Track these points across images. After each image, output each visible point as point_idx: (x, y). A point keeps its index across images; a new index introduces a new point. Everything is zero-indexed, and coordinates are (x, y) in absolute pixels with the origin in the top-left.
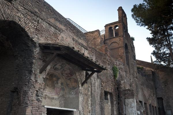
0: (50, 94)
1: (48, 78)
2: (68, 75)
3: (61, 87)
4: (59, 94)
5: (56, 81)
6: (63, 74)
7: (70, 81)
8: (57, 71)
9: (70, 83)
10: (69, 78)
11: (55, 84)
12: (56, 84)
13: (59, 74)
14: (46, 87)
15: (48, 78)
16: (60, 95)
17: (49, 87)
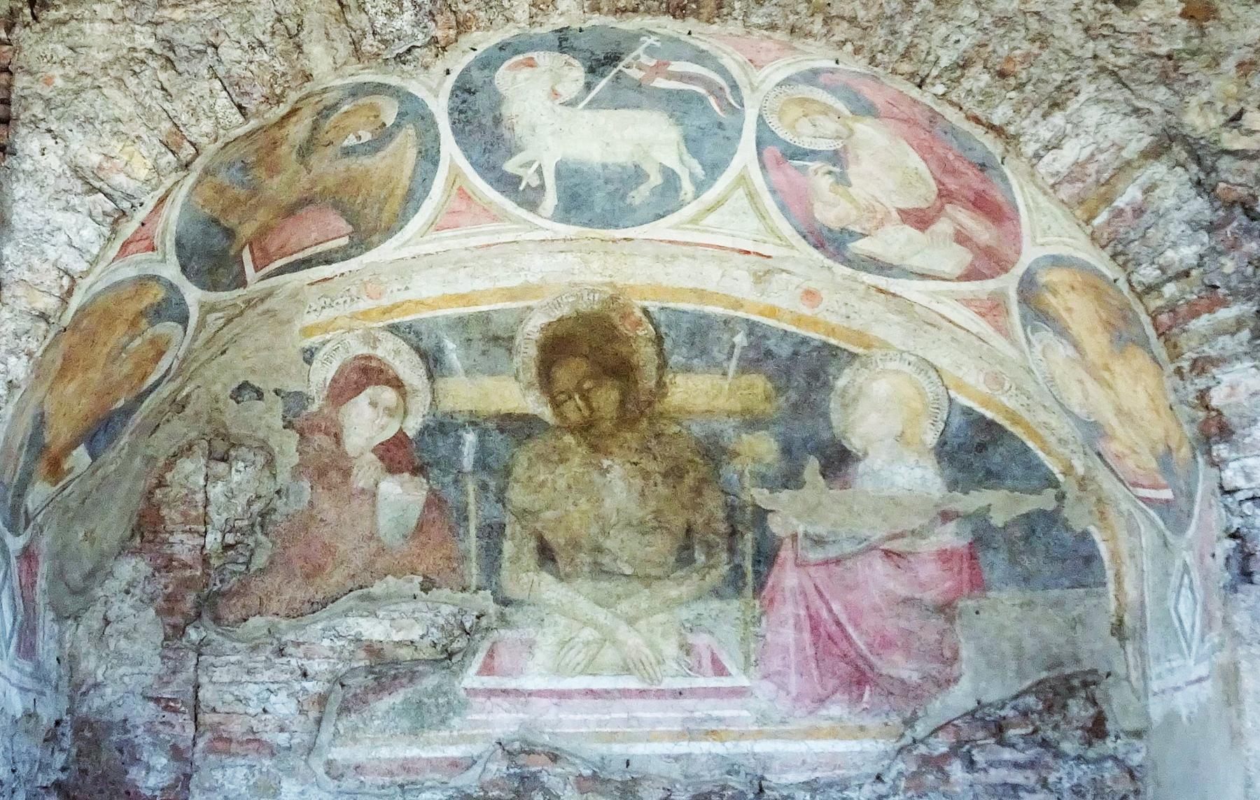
0: (648, 711)
1: (533, 403)
2: (962, 238)
3: (979, 519)
4: (904, 669)
5: (752, 422)
6: (860, 247)
7: (1071, 351)
8: (661, 229)
9: (1091, 385)
10: (1008, 283)
11: (761, 496)
12: (791, 479)
13: (760, 278)
14: (506, 602)
15: (533, 403)
16: (960, 698)
17: (599, 571)
